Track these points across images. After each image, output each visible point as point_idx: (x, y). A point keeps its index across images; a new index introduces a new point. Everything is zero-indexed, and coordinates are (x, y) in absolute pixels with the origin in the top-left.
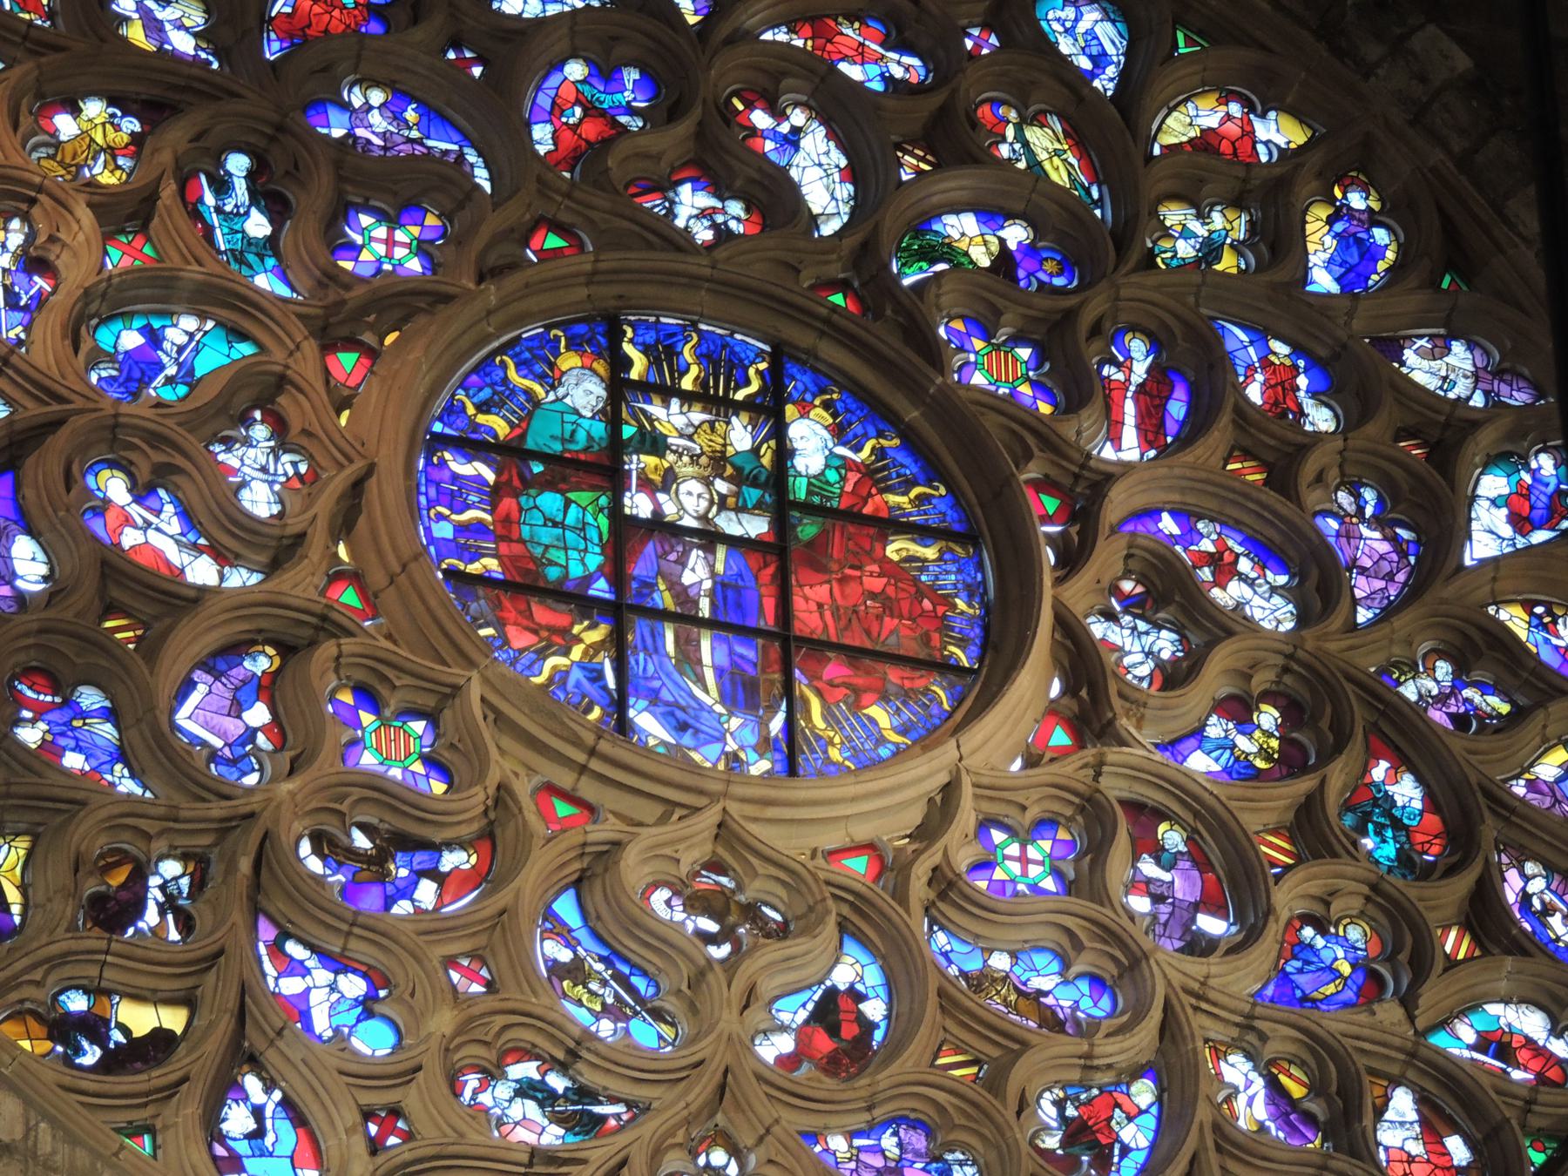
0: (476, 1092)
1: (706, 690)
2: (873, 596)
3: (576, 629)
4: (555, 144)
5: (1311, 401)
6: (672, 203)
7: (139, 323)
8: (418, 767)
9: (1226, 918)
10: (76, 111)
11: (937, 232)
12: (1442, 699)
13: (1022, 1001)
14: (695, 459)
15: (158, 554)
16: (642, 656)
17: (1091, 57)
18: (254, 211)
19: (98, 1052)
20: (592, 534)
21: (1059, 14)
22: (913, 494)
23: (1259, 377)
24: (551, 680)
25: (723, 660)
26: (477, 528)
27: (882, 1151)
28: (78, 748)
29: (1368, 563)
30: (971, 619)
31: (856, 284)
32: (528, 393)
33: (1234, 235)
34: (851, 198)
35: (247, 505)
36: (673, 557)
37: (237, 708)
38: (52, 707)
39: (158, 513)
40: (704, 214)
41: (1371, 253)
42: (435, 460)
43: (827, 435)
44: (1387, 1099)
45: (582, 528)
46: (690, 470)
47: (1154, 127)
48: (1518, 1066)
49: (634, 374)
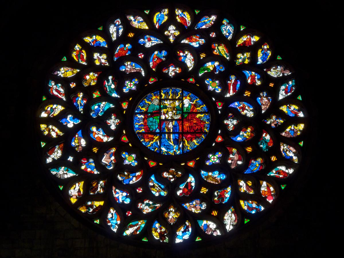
0: (140, 206)
1: (171, 143)
2: (195, 124)
3: (154, 137)
4: (153, 65)
5: (257, 80)
6: (169, 70)
7: (97, 104)
8: (133, 161)
9: (242, 161)
10: (89, 75)
11: (206, 66)
12: (273, 122)
13: (213, 179)
14: (171, 109)
15: (100, 138)
16: (163, 139)
17: (228, 33)
18: (112, 84)
19: (92, 209)
20: (157, 123)
21: (224, 27)
22: (200, 107)
23: (250, 78)
24: (151, 145)
25: (174, 138)
26: (142, 125)
27: (193, 204)
28: (89, 168)
29: (264, 103)
30: (208, 124)
31: (194, 77)
32: (148, 104)
33: (248, 57)
34: (193, 63)
35: (111, 128)
36: (167, 124)
37: (110, 157)
38: (86, 163)
39: (100, 132)
40: (173, 71)
41: (266, 55)
42: (136, 116)
43: (189, 101)
44: (262, 183)
45: (155, 122)
46: (170, 110)
47: (237, 42)
48: (281, 175)
49: (163, 98)
